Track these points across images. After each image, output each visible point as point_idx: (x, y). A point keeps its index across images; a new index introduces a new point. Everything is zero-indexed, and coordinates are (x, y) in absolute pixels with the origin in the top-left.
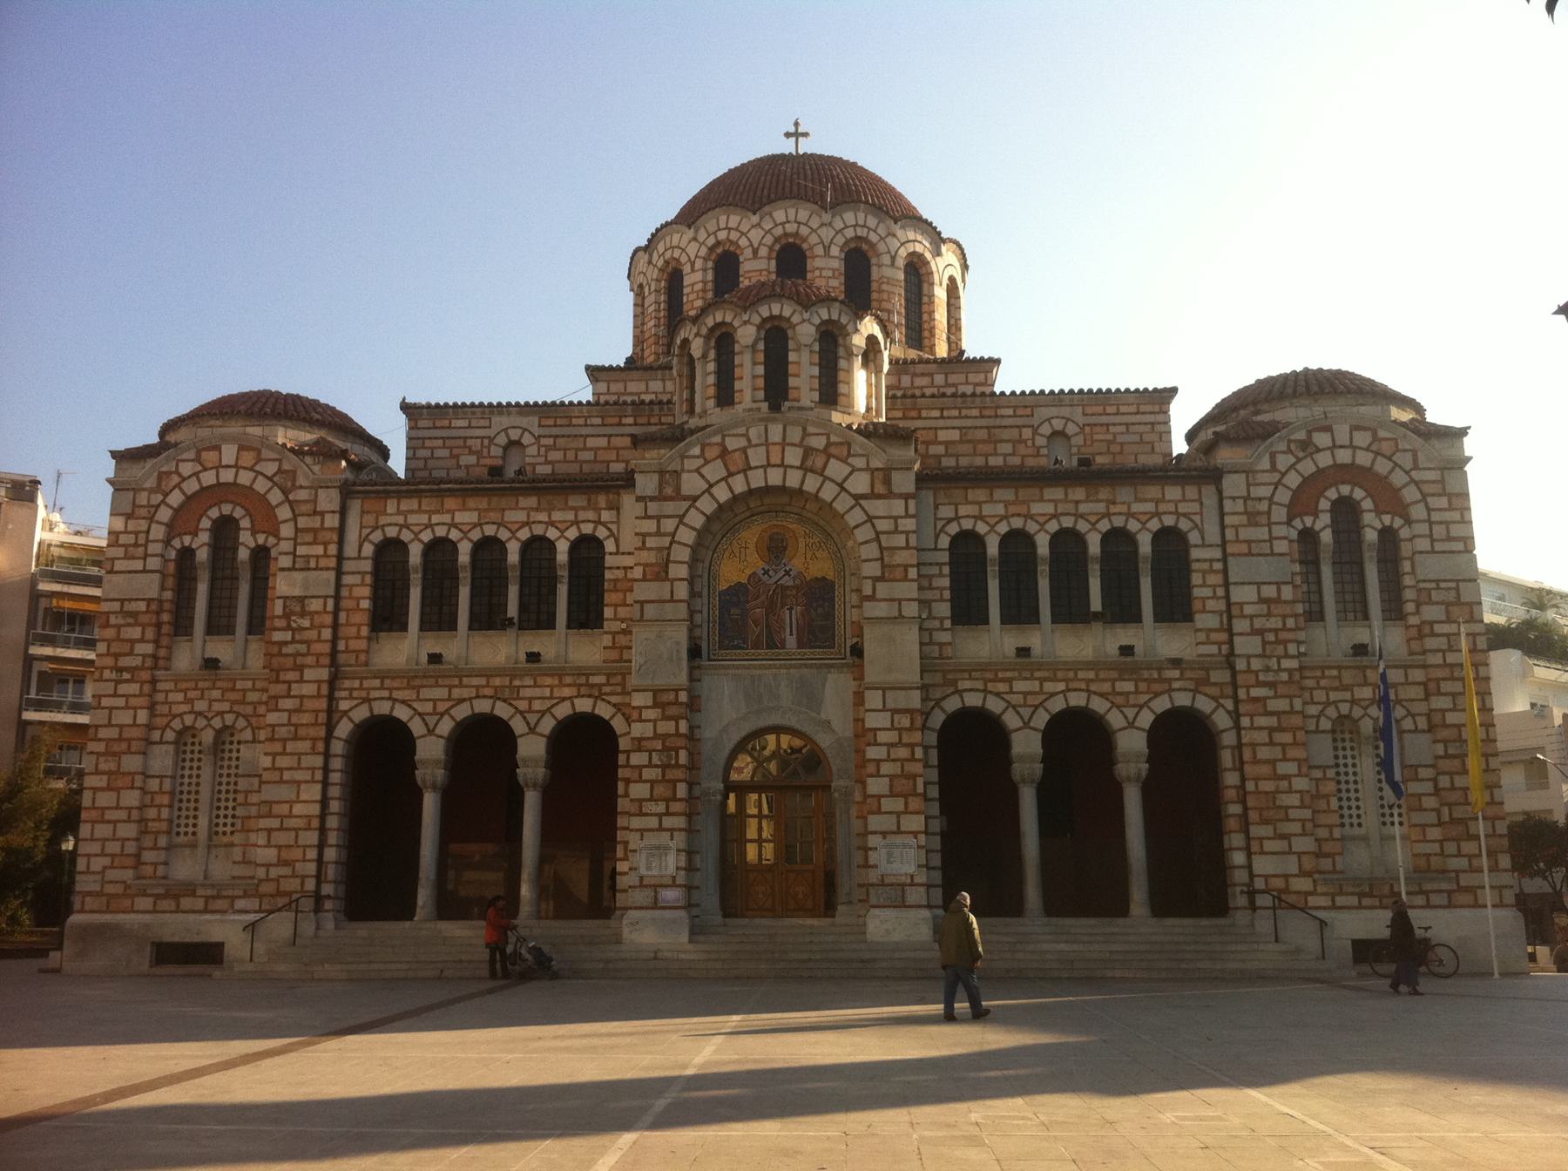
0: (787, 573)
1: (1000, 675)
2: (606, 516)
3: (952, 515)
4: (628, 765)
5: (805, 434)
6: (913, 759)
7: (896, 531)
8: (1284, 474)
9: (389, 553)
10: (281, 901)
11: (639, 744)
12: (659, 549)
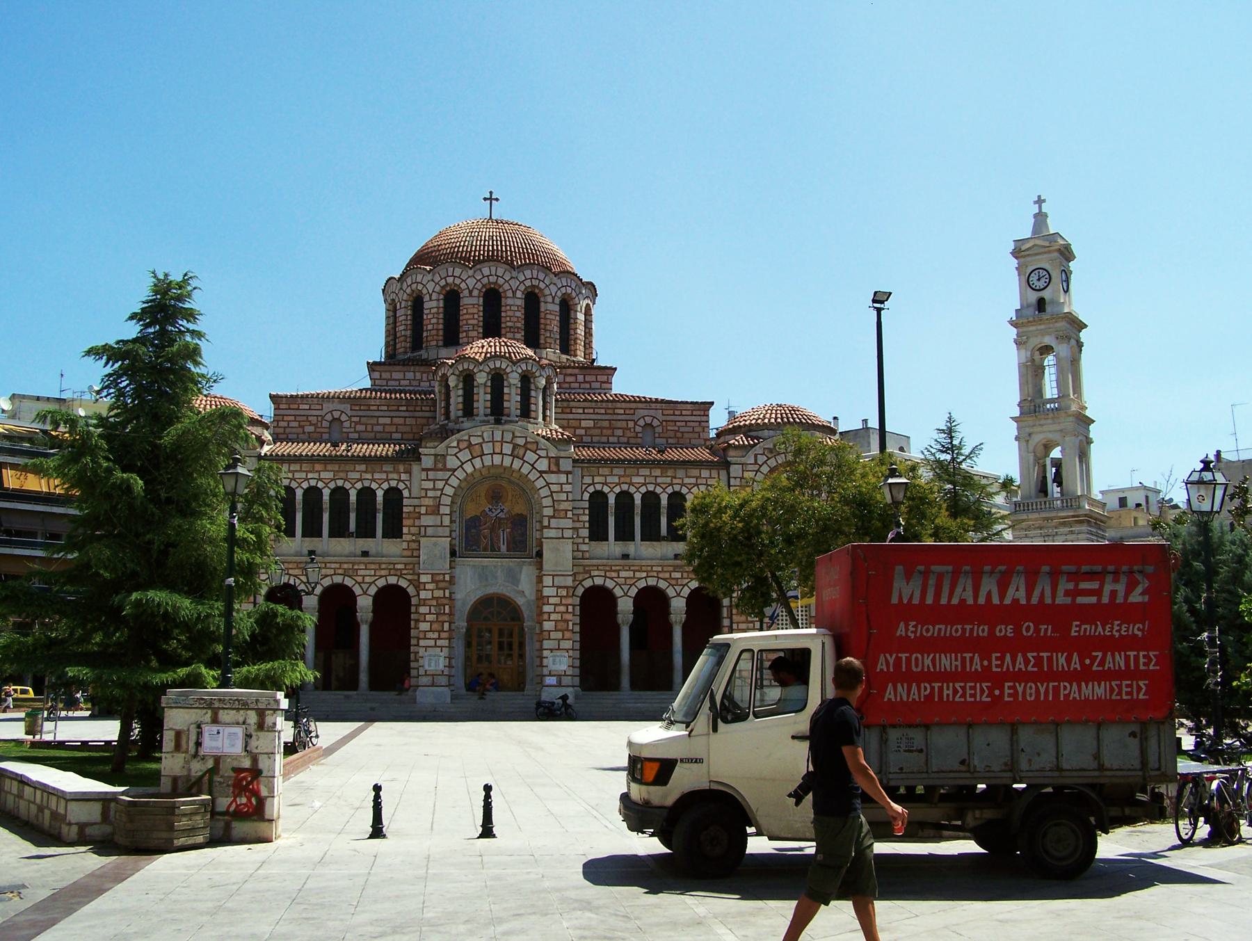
0: (502, 511)
1: (613, 568)
2: (403, 476)
3: (591, 482)
4: (417, 612)
6: (567, 612)
7: (561, 491)
8: (761, 466)
11: (423, 602)
12: (435, 498)
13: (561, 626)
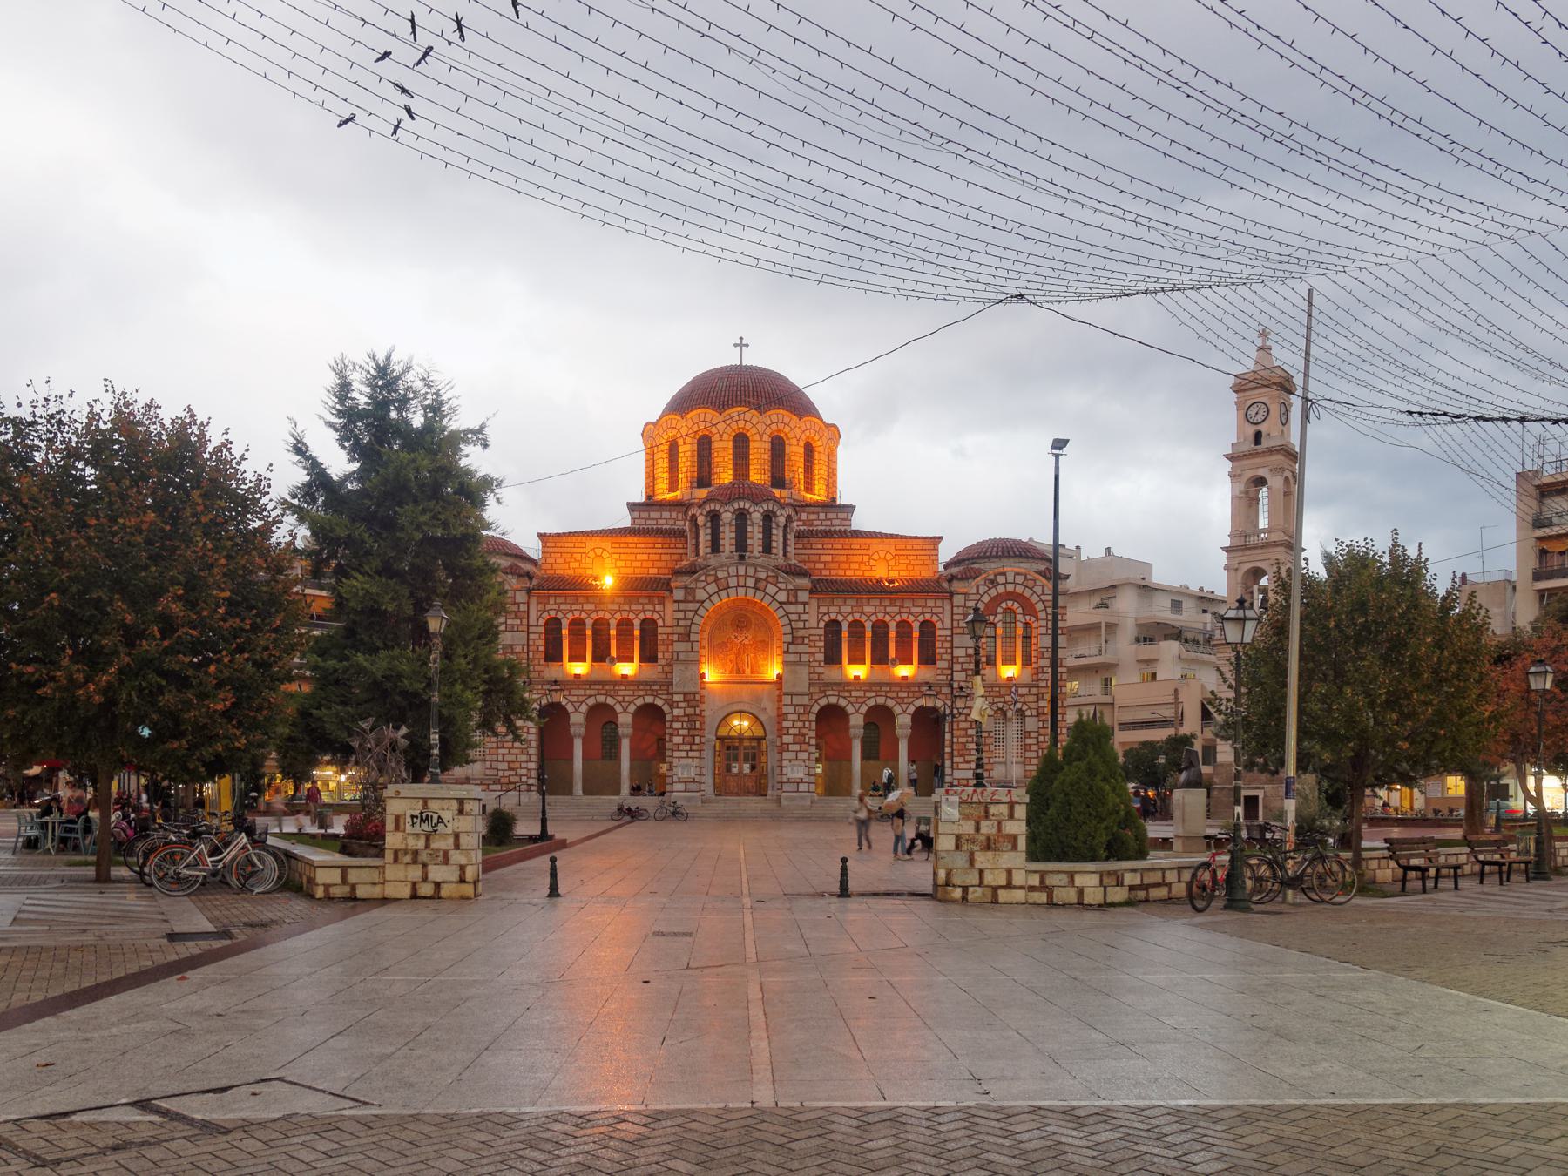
2: (658, 608)
4: (671, 728)
5: (756, 571)
7: (799, 620)
9: (553, 626)
10: (511, 787)
11: (677, 719)
13: (800, 739)
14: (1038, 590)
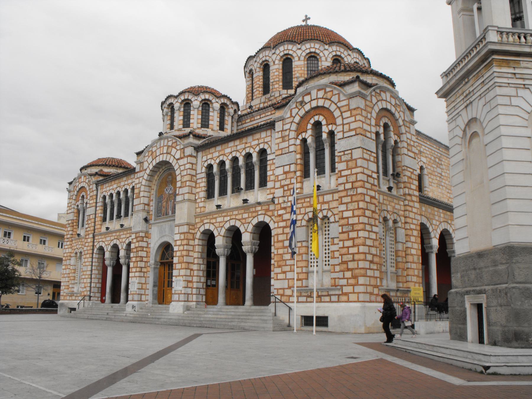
8: (294, 117)
14: (335, 99)
